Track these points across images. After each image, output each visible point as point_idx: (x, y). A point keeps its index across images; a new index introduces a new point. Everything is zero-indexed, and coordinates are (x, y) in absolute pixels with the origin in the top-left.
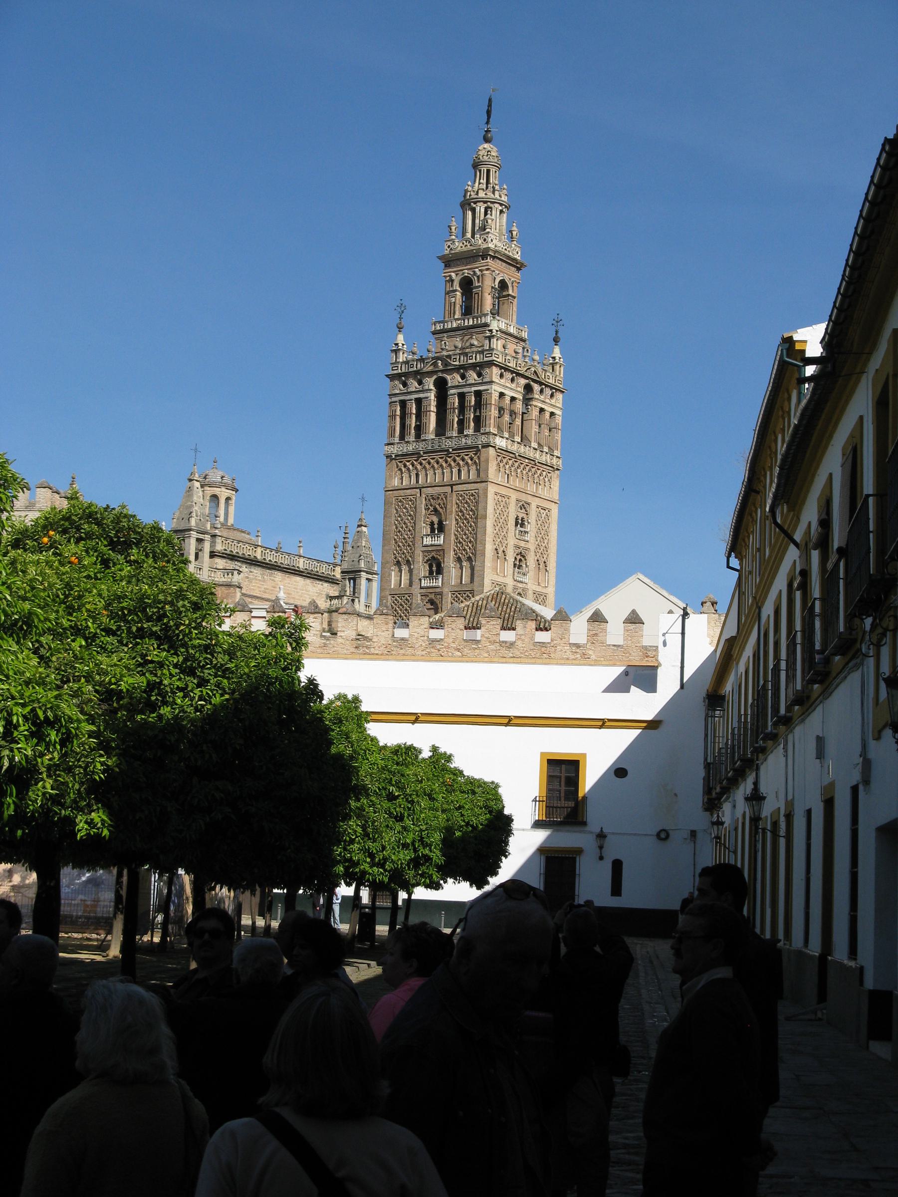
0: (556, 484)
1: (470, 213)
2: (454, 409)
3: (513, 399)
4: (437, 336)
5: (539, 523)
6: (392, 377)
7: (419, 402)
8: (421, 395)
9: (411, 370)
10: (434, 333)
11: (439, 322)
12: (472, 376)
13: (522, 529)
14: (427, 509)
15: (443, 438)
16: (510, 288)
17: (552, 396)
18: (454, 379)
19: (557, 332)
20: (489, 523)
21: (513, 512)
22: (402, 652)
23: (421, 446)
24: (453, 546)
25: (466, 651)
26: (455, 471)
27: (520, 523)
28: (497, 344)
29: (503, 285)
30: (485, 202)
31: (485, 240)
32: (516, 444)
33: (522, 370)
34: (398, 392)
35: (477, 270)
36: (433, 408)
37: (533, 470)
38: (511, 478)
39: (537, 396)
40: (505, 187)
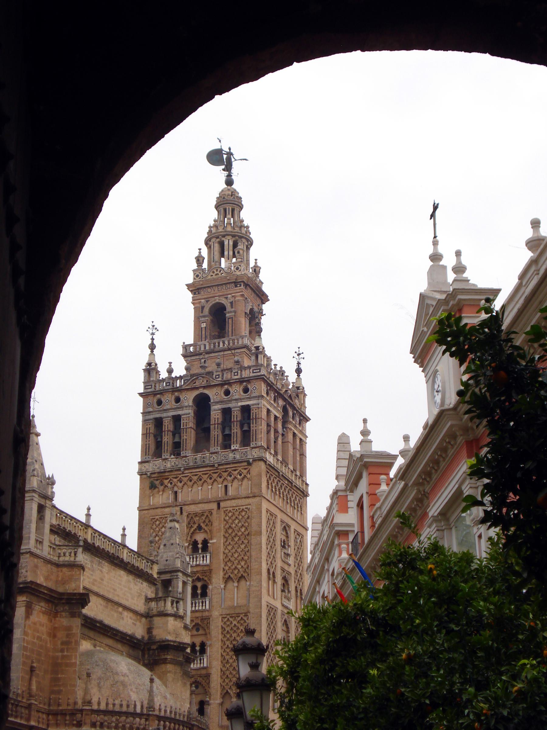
3: (276, 418)
8: (180, 412)
13: (286, 551)
18: (214, 394)
19: (299, 363)
30: (233, 236)
34: (151, 410)
35: (229, 296)
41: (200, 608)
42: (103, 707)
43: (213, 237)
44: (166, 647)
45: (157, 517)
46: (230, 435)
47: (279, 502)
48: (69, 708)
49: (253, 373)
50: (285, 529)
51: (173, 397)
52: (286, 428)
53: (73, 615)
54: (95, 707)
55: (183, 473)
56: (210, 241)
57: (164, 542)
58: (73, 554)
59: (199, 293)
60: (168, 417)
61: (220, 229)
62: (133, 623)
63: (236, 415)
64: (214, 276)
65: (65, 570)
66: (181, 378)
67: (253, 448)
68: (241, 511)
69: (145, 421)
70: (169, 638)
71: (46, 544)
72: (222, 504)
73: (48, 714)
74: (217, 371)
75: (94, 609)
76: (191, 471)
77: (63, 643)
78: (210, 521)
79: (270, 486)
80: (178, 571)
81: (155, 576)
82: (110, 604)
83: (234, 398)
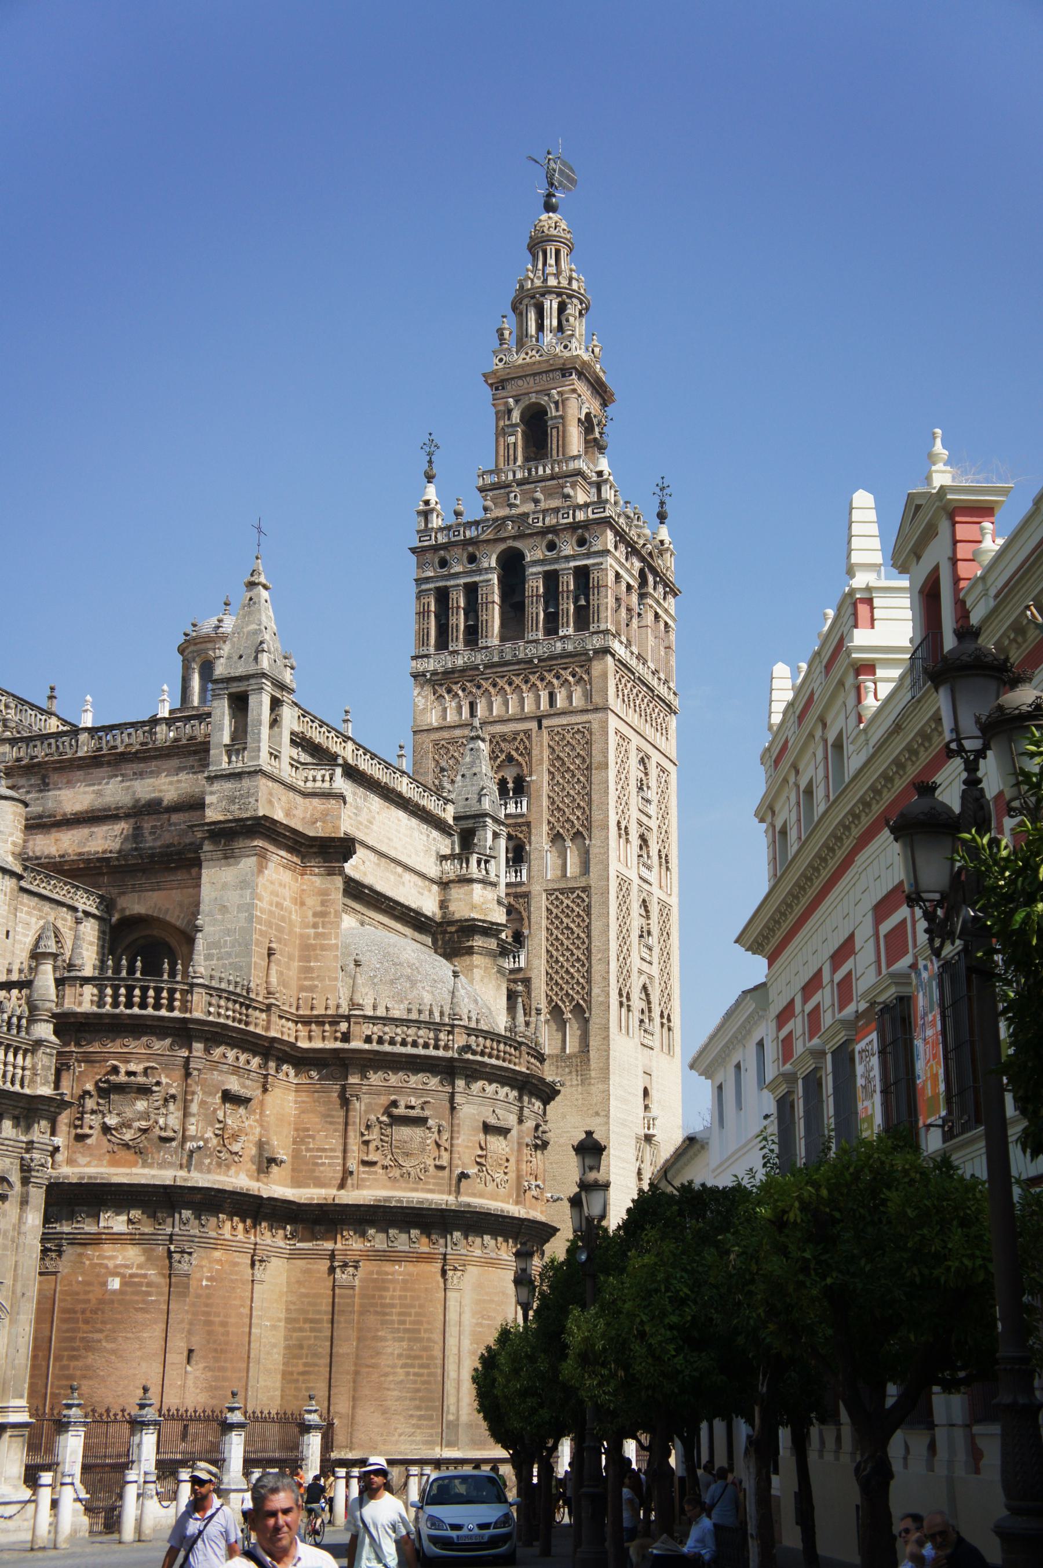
2: (537, 596)
3: (629, 587)
7: (471, 590)
8: (477, 579)
9: (453, 539)
10: (481, 490)
11: (491, 472)
13: (645, 795)
19: (662, 503)
23: (479, 658)
24: (546, 815)
26: (544, 695)
30: (559, 294)
31: (566, 347)
34: (432, 574)
35: (554, 392)
42: (381, 1012)
43: (527, 296)
44: (471, 928)
45: (443, 742)
46: (556, 613)
47: (634, 718)
48: (329, 1012)
49: (593, 513)
50: (642, 761)
51: (465, 555)
53: (331, 873)
54: (369, 1012)
55: (482, 673)
56: (521, 303)
57: (463, 770)
58: (327, 778)
59: (503, 388)
60: (458, 586)
61: (538, 283)
62: (419, 892)
63: (568, 583)
64: (528, 360)
65: (316, 801)
66: (477, 523)
67: (594, 633)
68: (576, 733)
69: (420, 595)
70: (474, 915)
71: (285, 760)
72: (545, 723)
73: (296, 1023)
74: (534, 513)
75: (360, 866)
76: (495, 670)
77: (315, 915)
78: (526, 748)
79: (620, 694)
80: (486, 815)
81: (451, 822)
82: (383, 860)
83: (563, 554)
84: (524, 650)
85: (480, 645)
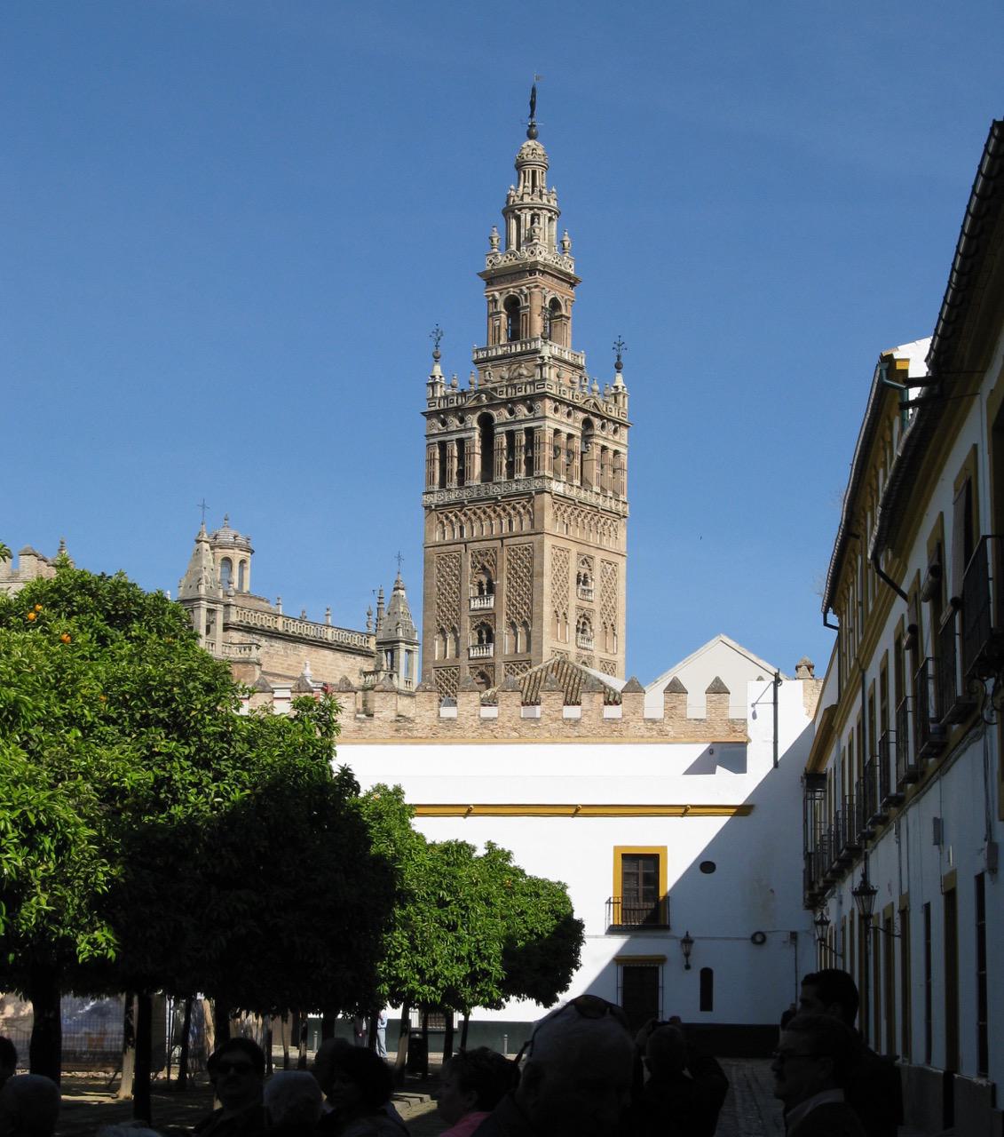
0: (623, 534)
1: (514, 222)
2: (502, 450)
3: (570, 436)
4: (479, 366)
5: (605, 579)
6: (429, 415)
7: (461, 442)
8: (463, 435)
10: (476, 362)
11: (482, 350)
12: (522, 411)
14: (474, 567)
15: (490, 484)
16: (563, 307)
17: (615, 431)
18: (500, 416)
19: (619, 357)
20: (547, 581)
21: (574, 567)
22: (449, 734)
23: (465, 494)
25: (524, 730)
26: (505, 521)
27: (582, 580)
28: (550, 374)
29: (555, 304)
30: (531, 209)
31: (532, 253)
32: (575, 489)
33: (580, 403)
34: (436, 432)
35: (524, 288)
36: (478, 450)
37: (596, 518)
38: (571, 529)
39: (597, 432)
40: (554, 190)
41: (485, 654)
47: (576, 533)
52: (591, 443)
67: (536, 478)
83: (517, 419)
84: (495, 491)
85: (466, 485)
